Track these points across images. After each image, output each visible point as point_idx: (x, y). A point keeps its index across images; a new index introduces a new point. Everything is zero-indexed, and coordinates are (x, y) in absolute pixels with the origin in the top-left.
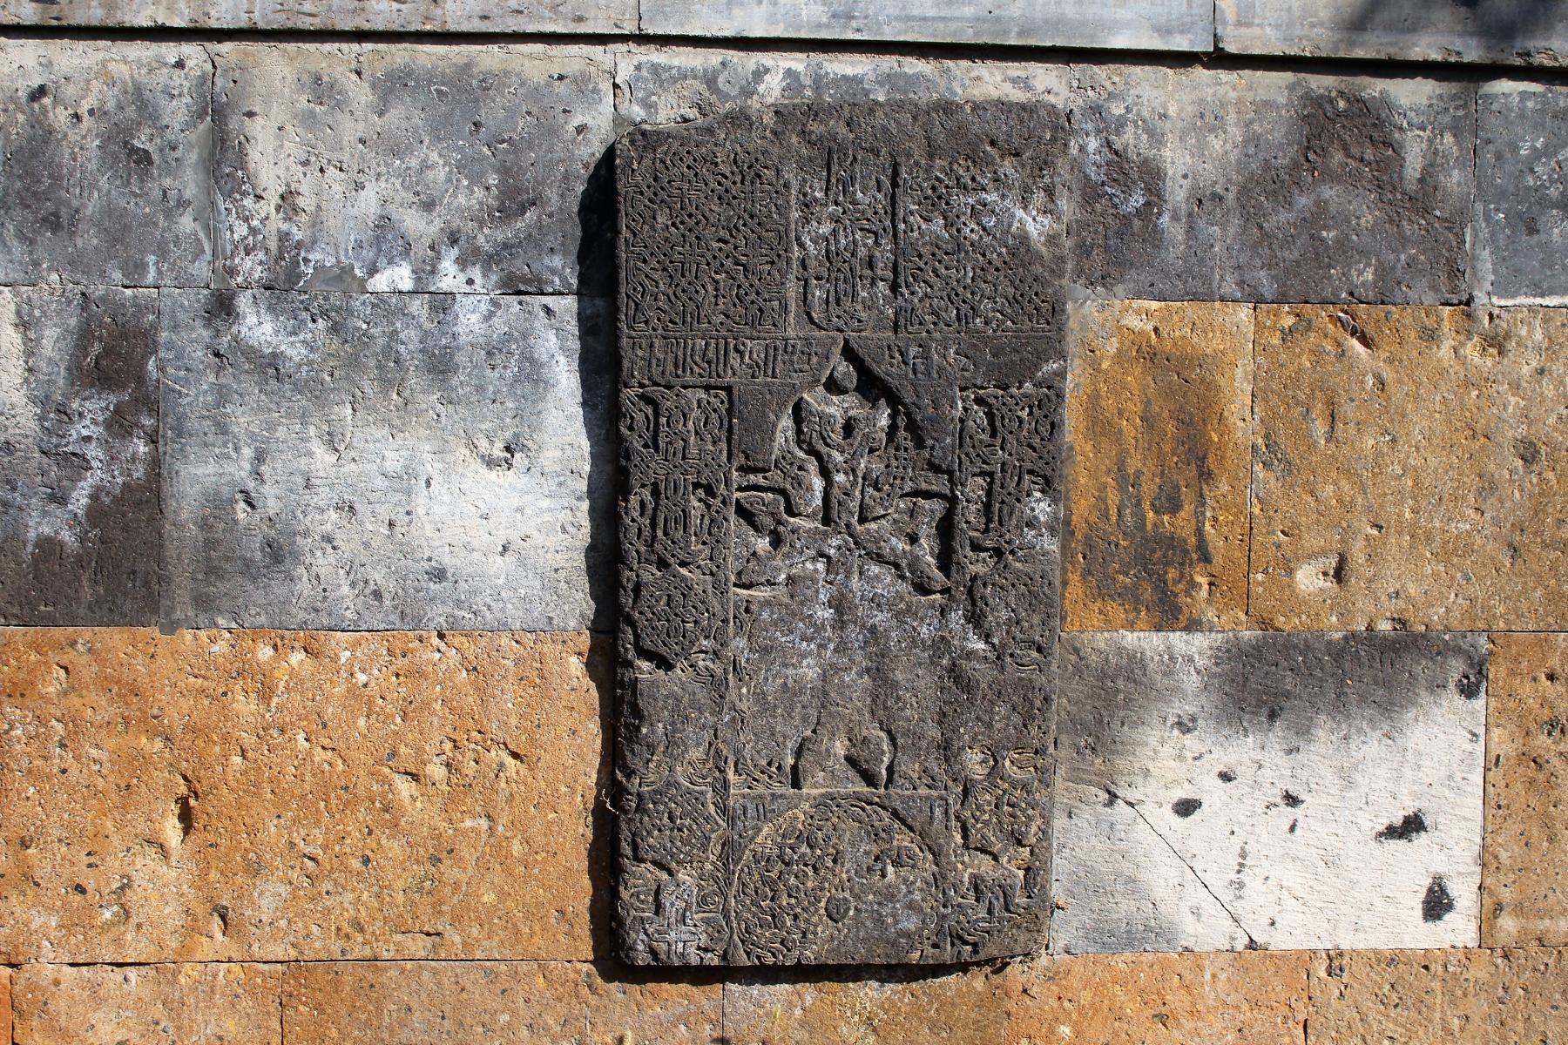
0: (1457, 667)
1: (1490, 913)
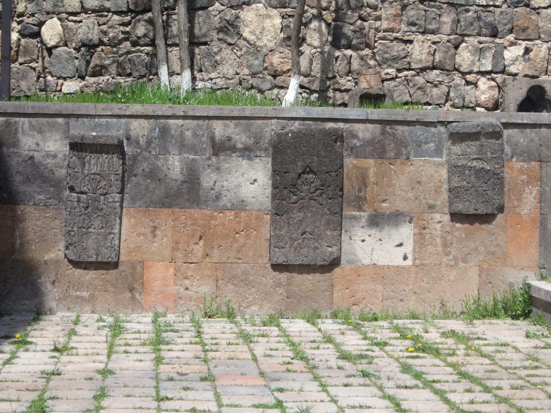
0: (408, 218)
1: (415, 259)
